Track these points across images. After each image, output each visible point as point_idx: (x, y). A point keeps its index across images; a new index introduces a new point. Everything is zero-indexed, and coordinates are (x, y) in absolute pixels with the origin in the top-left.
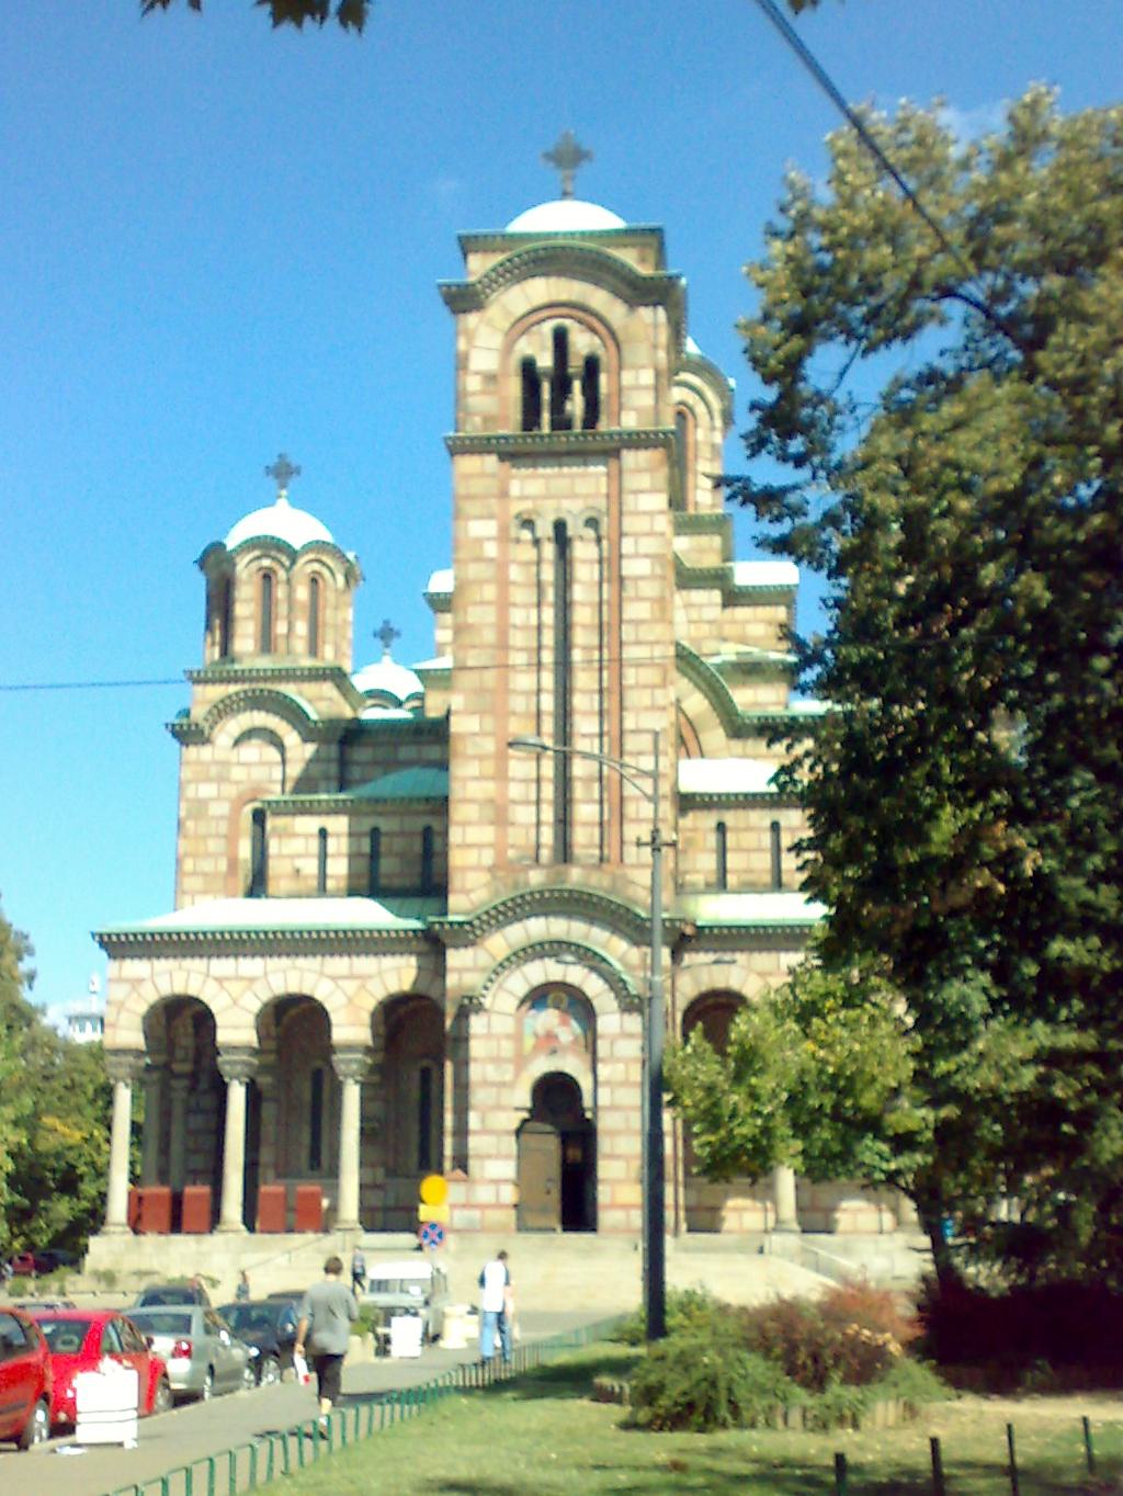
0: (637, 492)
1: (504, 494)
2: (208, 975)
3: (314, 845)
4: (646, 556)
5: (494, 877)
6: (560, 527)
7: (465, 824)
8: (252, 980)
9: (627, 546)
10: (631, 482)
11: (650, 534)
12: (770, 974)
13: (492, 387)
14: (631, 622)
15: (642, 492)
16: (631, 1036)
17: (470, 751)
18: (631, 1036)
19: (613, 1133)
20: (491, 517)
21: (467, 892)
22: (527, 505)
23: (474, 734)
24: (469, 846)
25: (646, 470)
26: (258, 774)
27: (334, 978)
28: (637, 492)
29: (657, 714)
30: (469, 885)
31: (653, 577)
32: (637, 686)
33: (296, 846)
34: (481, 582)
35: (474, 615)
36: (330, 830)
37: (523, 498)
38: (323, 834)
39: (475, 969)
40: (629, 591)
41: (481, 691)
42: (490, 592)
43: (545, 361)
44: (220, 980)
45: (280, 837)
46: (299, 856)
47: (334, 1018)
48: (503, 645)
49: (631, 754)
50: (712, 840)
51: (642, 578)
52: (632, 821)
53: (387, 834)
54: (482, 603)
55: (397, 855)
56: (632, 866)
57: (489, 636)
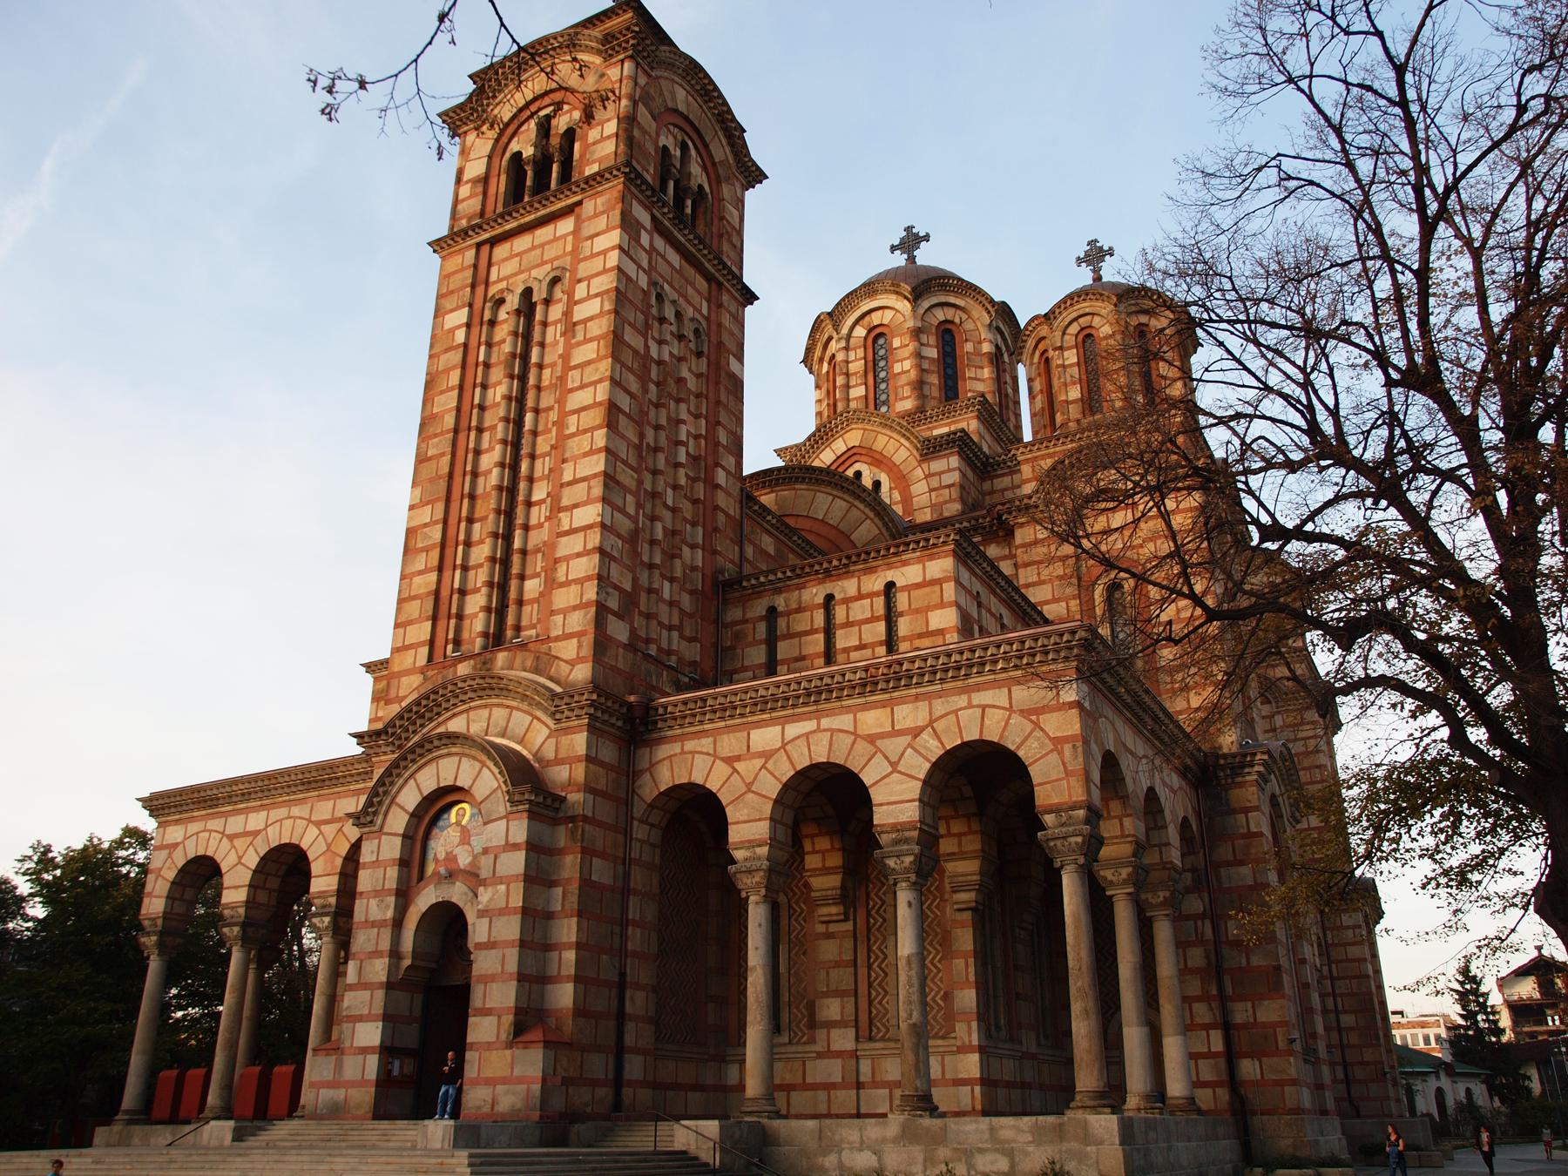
0: (592, 237)
4: (597, 295)
6: (528, 292)
8: (255, 833)
10: (588, 229)
12: (738, 758)
14: (575, 367)
15: (597, 235)
16: (515, 847)
17: (420, 545)
18: (515, 847)
19: (488, 979)
22: (503, 285)
23: (426, 525)
25: (603, 213)
27: (318, 824)
28: (592, 237)
29: (595, 457)
31: (601, 314)
32: (579, 432)
37: (500, 280)
40: (580, 337)
44: (231, 837)
47: (316, 868)
50: (762, 628)
51: (591, 319)
52: (562, 585)
56: (557, 639)
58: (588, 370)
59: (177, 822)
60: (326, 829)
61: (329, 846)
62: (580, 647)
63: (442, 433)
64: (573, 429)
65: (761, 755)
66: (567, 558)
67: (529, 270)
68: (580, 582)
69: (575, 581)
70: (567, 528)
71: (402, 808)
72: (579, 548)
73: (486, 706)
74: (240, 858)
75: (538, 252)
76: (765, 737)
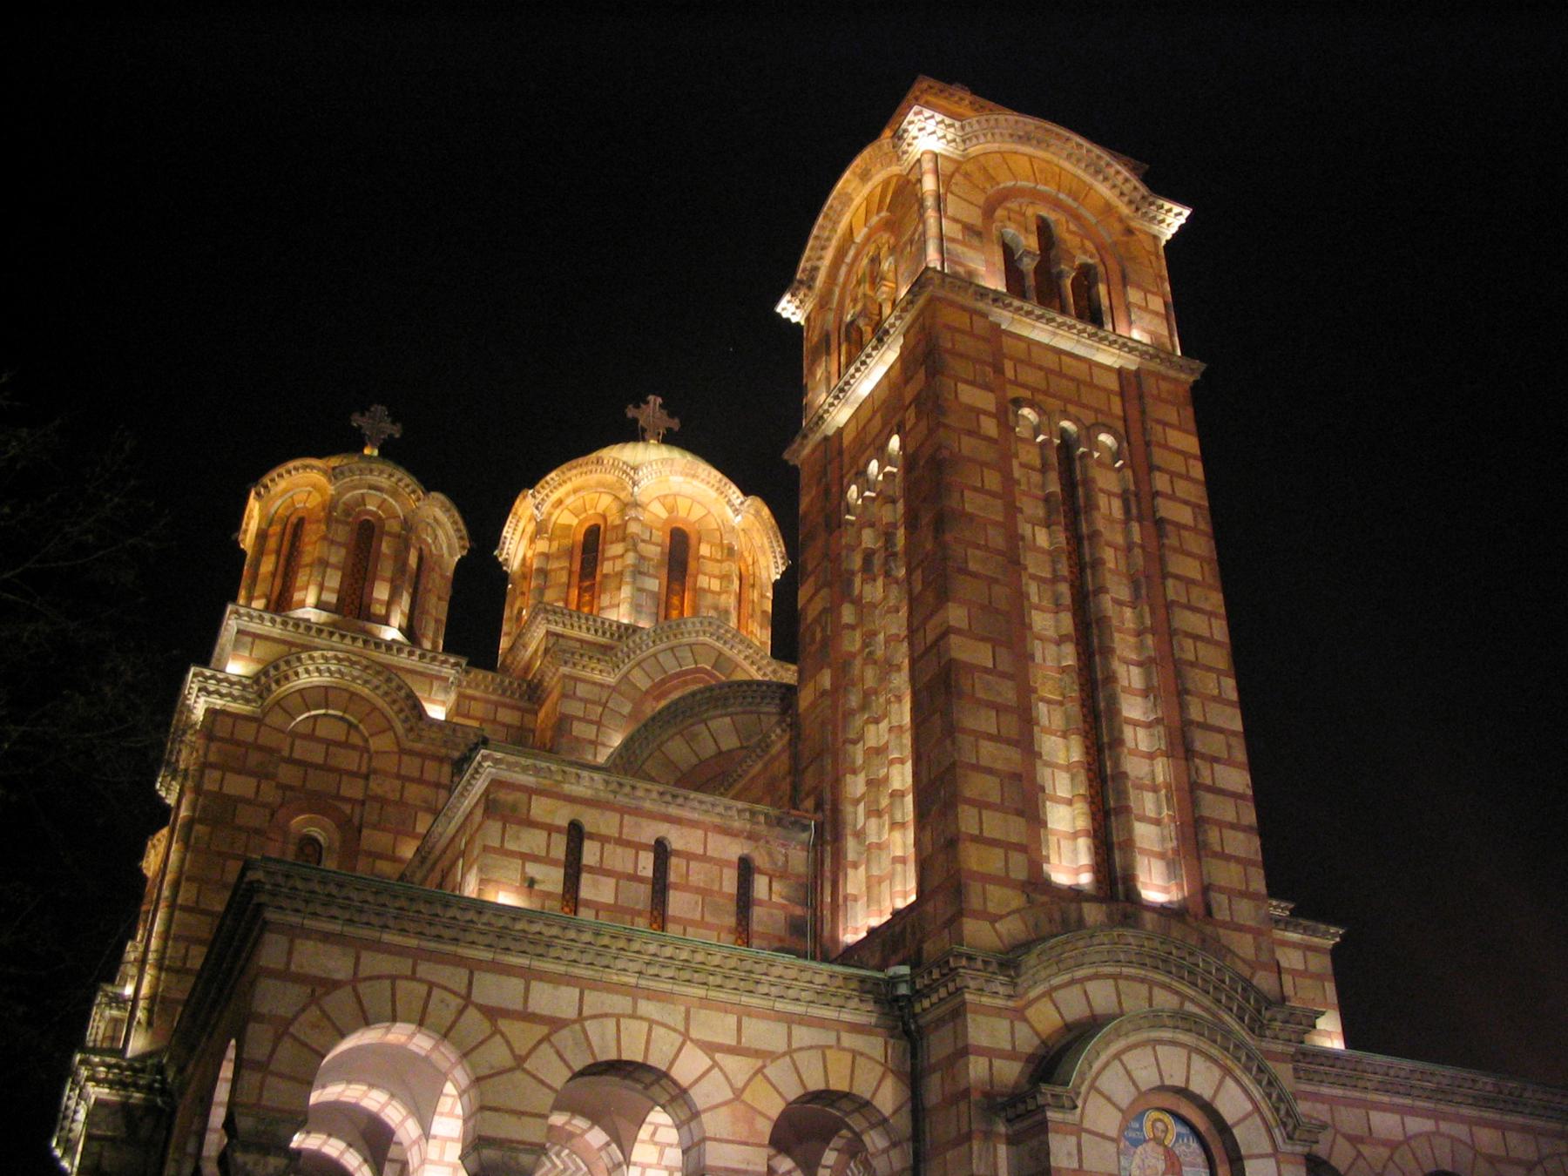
0: (1165, 424)
1: (999, 370)
2: (467, 998)
3: (559, 850)
5: (1029, 900)
7: (982, 805)
8: (556, 1024)
9: (1161, 482)
11: (1188, 478)
13: (976, 242)
14: (1177, 577)
15: (1171, 426)
17: (980, 694)
20: (987, 387)
21: (994, 919)
23: (986, 670)
24: (993, 843)
26: (316, 782)
27: (710, 1048)
30: (991, 908)
33: (533, 841)
34: (984, 464)
35: (973, 503)
36: (588, 828)
37: (1016, 383)
38: (576, 834)
39: (1012, 1055)
40: (1172, 541)
41: (988, 608)
42: (993, 481)
43: (1031, 242)
44: (492, 1013)
45: (505, 821)
46: (535, 859)
48: (1013, 561)
49: (1203, 756)
51: (1185, 527)
52: (1215, 855)
53: (678, 853)
54: (982, 490)
55: (697, 890)
57: (997, 539)
58: (1196, 592)
59: (326, 937)
60: (729, 1062)
61: (738, 1094)
62: (1258, 949)
63: (986, 548)
64: (1190, 656)
65: (1386, 1143)
66: (1221, 824)
67: (1067, 401)
68: (1244, 862)
69: (1238, 860)
70: (1208, 782)
71: (1109, 1099)
72: (1230, 816)
73: (1143, 980)
74: (520, 1060)
75: (1072, 386)
76: (1385, 1123)
